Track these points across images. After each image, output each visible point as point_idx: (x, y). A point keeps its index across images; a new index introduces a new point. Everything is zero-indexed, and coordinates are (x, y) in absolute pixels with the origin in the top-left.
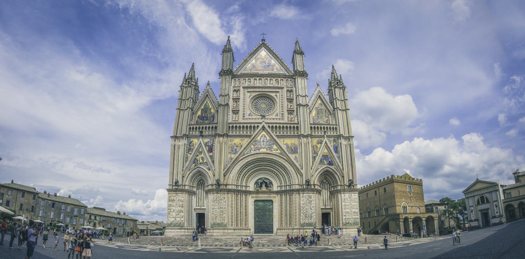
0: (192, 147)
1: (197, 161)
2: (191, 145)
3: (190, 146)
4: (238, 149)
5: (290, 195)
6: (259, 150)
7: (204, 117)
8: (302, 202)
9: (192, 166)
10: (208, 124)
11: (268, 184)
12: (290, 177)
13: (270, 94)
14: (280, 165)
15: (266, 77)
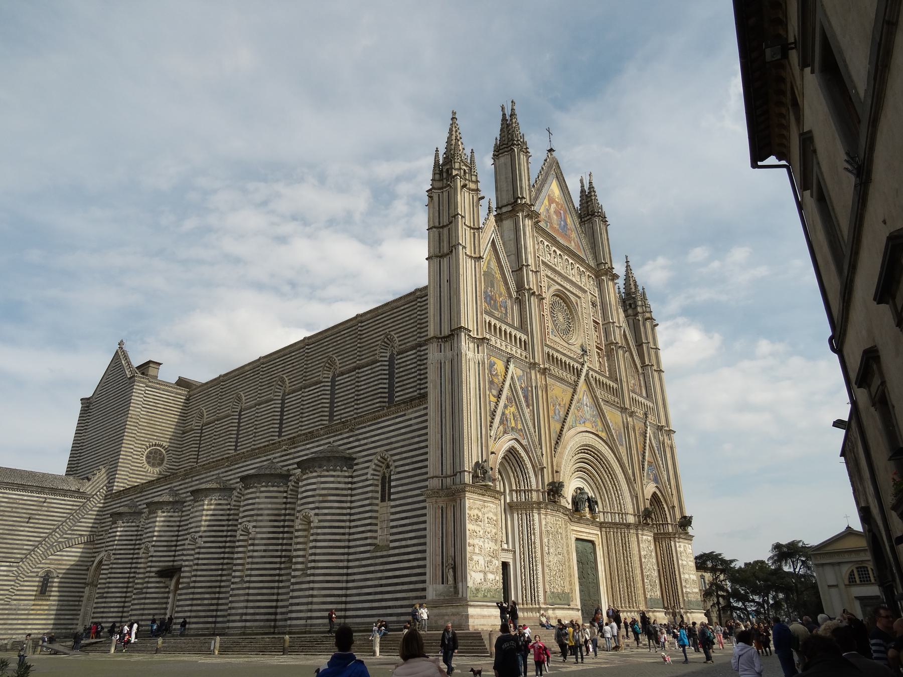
0: (496, 380)
1: (507, 420)
2: (494, 373)
3: (492, 375)
4: (561, 413)
5: (623, 534)
6: (584, 422)
7: (491, 298)
8: (642, 553)
9: (499, 429)
10: (497, 318)
11: (592, 503)
12: (620, 497)
13: (572, 298)
14: (607, 468)
15: (558, 248)
